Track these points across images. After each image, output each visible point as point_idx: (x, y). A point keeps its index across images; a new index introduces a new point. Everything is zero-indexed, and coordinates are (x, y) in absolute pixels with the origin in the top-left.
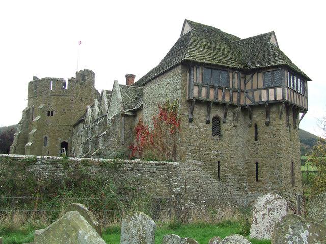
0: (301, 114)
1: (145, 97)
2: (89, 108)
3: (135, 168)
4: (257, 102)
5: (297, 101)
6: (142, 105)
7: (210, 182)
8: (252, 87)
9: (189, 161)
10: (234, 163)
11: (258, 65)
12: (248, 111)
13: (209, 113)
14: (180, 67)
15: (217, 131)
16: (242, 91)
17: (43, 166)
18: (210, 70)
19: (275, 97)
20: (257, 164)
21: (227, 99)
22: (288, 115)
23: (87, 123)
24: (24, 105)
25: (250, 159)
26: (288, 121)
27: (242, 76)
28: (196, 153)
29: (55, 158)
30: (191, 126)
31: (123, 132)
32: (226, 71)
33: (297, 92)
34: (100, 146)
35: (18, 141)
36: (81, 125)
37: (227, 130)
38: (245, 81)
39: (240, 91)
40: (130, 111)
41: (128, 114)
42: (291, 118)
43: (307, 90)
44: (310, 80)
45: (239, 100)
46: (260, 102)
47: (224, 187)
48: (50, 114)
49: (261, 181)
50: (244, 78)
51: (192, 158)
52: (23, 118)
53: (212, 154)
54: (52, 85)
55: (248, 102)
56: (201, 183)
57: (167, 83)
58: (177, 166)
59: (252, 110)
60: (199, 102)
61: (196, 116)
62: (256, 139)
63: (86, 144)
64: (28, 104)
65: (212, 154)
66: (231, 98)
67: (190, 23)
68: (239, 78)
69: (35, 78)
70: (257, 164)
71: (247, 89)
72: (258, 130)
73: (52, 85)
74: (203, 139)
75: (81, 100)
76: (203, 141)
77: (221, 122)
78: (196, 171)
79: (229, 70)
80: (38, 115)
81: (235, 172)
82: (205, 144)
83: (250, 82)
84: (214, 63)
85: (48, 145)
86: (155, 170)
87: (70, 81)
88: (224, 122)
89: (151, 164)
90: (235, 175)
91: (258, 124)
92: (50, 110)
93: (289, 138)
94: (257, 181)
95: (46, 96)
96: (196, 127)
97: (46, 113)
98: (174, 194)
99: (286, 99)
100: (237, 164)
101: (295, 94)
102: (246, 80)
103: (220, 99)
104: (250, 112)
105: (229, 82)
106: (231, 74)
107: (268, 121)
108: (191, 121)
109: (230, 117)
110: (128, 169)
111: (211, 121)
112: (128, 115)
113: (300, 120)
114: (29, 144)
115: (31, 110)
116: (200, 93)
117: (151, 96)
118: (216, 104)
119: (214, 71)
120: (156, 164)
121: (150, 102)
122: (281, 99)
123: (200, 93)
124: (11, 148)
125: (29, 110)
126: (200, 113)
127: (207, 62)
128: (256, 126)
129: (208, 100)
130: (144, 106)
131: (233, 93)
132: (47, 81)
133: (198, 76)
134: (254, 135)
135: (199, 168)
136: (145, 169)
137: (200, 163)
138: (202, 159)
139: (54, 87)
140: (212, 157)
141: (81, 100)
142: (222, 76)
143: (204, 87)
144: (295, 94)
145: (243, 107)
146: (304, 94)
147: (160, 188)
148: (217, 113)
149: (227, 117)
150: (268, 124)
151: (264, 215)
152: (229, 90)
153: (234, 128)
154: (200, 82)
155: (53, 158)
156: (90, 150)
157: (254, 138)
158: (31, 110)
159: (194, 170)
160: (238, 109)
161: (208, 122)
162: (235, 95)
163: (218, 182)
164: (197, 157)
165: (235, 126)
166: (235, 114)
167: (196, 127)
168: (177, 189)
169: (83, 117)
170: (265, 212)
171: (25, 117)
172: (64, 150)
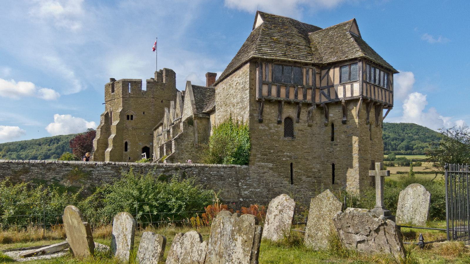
0: (385, 111)
1: (218, 98)
2: (166, 110)
3: (202, 172)
4: (333, 100)
5: (379, 96)
6: (215, 107)
7: (282, 185)
8: (328, 84)
9: (259, 164)
10: (309, 165)
11: (334, 59)
12: (323, 109)
13: (280, 112)
14: (248, 65)
15: (289, 131)
16: (317, 88)
17: (105, 172)
18: (281, 67)
19: (352, 93)
20: (333, 165)
21: (300, 97)
22: (368, 112)
23: (165, 126)
25: (326, 160)
26: (368, 119)
27: (317, 72)
28: (266, 155)
29: (117, 163)
30: (261, 127)
31: (196, 135)
32: (299, 67)
33: (378, 87)
34: (173, 151)
35: (97, 147)
36: (160, 128)
37: (301, 130)
38: (320, 77)
39: (314, 88)
40: (204, 113)
41: (201, 116)
42: (372, 114)
43: (392, 84)
44: (397, 72)
45: (313, 98)
46: (336, 99)
47: (297, 190)
48: (130, 118)
49: (337, 184)
50: (320, 74)
51: (263, 160)
52: (101, 123)
53: (284, 156)
54: (130, 87)
55: (324, 100)
56: (272, 186)
57: (236, 82)
58: (246, 169)
59: (328, 109)
60: (269, 101)
61: (266, 117)
62: (333, 139)
63: (161, 148)
64: (106, 108)
65: (284, 156)
66: (305, 96)
67: (263, 15)
68: (314, 74)
69: (113, 80)
70: (333, 165)
71: (323, 85)
72: (335, 130)
73: (130, 87)
74: (274, 140)
75: (162, 102)
76: (274, 143)
77: (294, 122)
78: (266, 174)
79: (302, 66)
81: (310, 174)
82: (277, 145)
83: (326, 77)
84: (285, 59)
85: (128, 150)
86: (222, 173)
88: (298, 122)
89: (219, 168)
90: (310, 177)
91: (335, 124)
92: (128, 114)
93: (369, 138)
94: (333, 183)
96: (267, 128)
97: (126, 117)
98: (243, 198)
99: (365, 94)
100: (312, 166)
101: (376, 88)
102: (322, 77)
103: (292, 97)
104: (326, 111)
105: (302, 79)
106: (304, 71)
107: (345, 119)
108: (261, 121)
109: (304, 116)
110: (194, 173)
111: (283, 121)
112: (201, 117)
113: (385, 117)
114: (109, 149)
115: (110, 114)
116: (270, 92)
117: (222, 97)
118: (289, 103)
119: (285, 67)
120: (223, 167)
121: (222, 103)
122: (358, 95)
123: (270, 92)
125: (107, 114)
126: (270, 111)
127: (278, 58)
128: (333, 125)
129: (279, 99)
130: (216, 108)
131: (306, 91)
132: (125, 83)
133: (267, 74)
134: (330, 135)
135: (270, 170)
136: (211, 173)
137: (271, 165)
138: (272, 162)
139: (132, 89)
140: (284, 159)
141: (162, 102)
142: (293, 73)
143: (274, 85)
144: (376, 88)
145: (318, 105)
146: (389, 89)
147: (228, 191)
148: (290, 112)
149: (301, 116)
150: (344, 123)
151: (275, 216)
152: (302, 88)
153: (309, 128)
154: (270, 80)
155: (115, 164)
156: (165, 154)
157: (330, 138)
158: (110, 114)
159: (264, 173)
160: (313, 108)
161: (279, 122)
162: (310, 92)
163: (290, 185)
164: (267, 160)
165: (310, 126)
166: (309, 113)
167: (267, 128)
168: (246, 192)
169: (159, 120)
170: (277, 213)
171: (103, 121)
172: (144, 155)
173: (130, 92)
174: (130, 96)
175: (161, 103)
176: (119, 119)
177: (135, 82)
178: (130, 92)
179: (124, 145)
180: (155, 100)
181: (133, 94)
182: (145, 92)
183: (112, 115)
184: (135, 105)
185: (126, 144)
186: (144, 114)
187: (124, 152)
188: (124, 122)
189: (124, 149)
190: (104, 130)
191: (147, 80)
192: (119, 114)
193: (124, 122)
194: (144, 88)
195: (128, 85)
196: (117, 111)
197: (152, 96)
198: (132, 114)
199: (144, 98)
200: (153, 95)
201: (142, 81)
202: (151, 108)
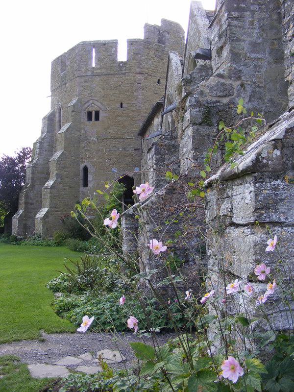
24: (45, 107)
35: (32, 179)
52: (42, 133)
54: (94, 54)
73: (94, 54)
75: (159, 82)
80: (67, 122)
85: (90, 185)
87: (131, 43)
92: (90, 109)
95: (83, 79)
97: (85, 116)
114: (50, 183)
115: (57, 115)
124: (21, 194)
139: (99, 60)
141: (159, 82)
158: (57, 115)
173: (94, 65)
174: (93, 72)
175: (156, 85)
176: (71, 118)
177: (105, 44)
178: (94, 65)
179: (81, 174)
180: (146, 79)
181: (101, 68)
182: (124, 63)
183: (61, 116)
184: (103, 89)
185: (86, 170)
186: (121, 107)
187: (82, 189)
188: (82, 126)
189: (81, 182)
190: (46, 145)
191: (128, 40)
192: (71, 109)
193: (82, 126)
194: (122, 55)
195: (90, 52)
196: (69, 105)
197: (138, 70)
198: (97, 109)
199: (121, 76)
200: (139, 67)
201: (117, 42)
202: (135, 94)
